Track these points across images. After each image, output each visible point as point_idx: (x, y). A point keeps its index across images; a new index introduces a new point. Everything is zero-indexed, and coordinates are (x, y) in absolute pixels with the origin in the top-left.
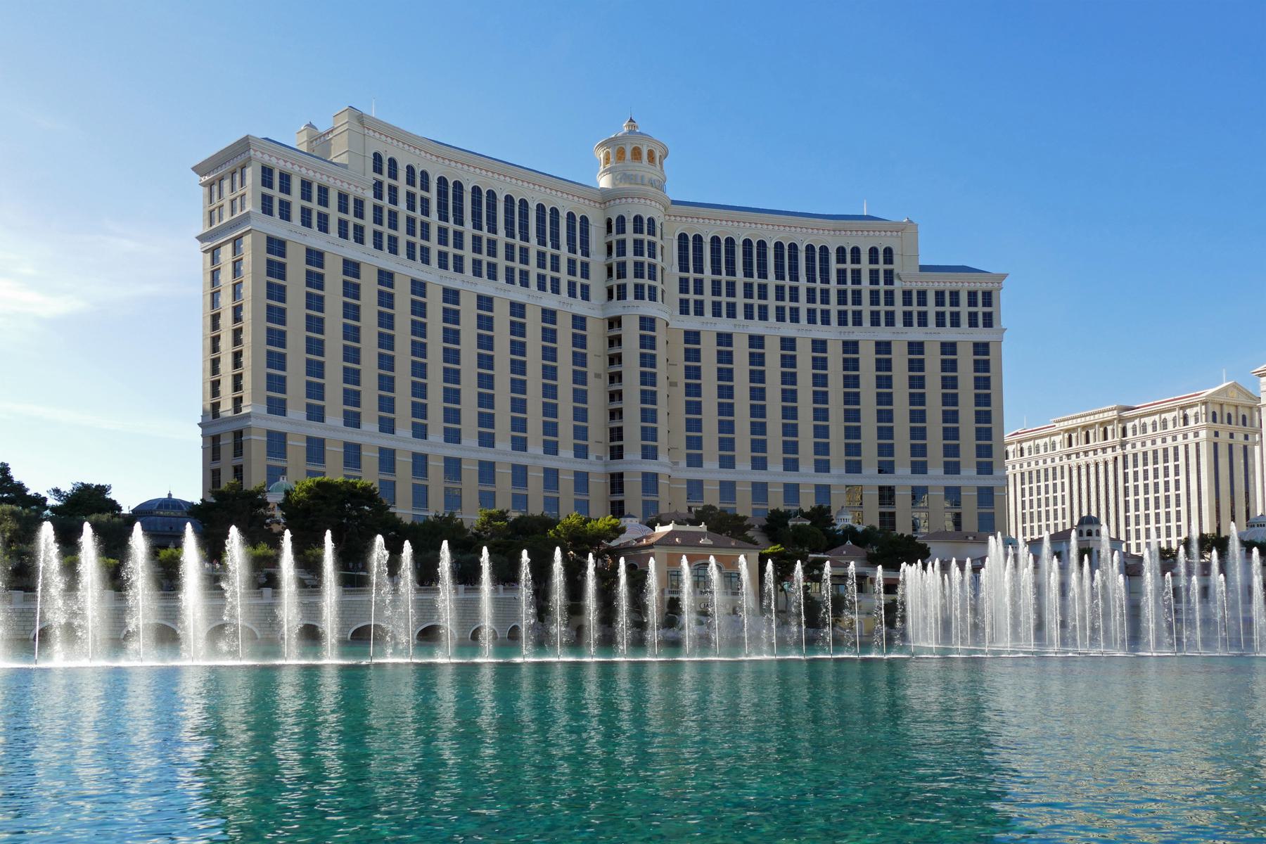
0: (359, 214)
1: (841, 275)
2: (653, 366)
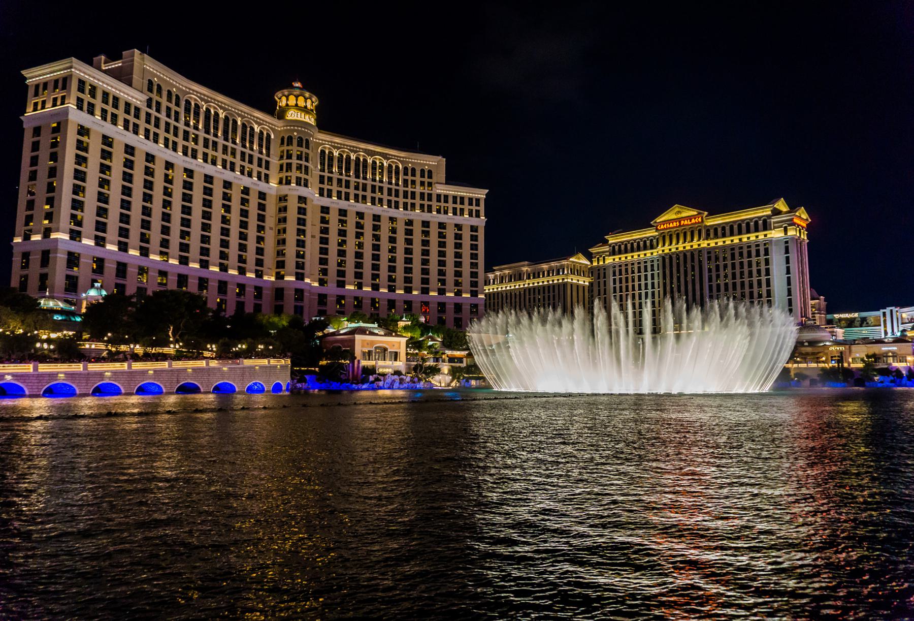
0: (137, 116)
1: (405, 182)
2: (304, 225)
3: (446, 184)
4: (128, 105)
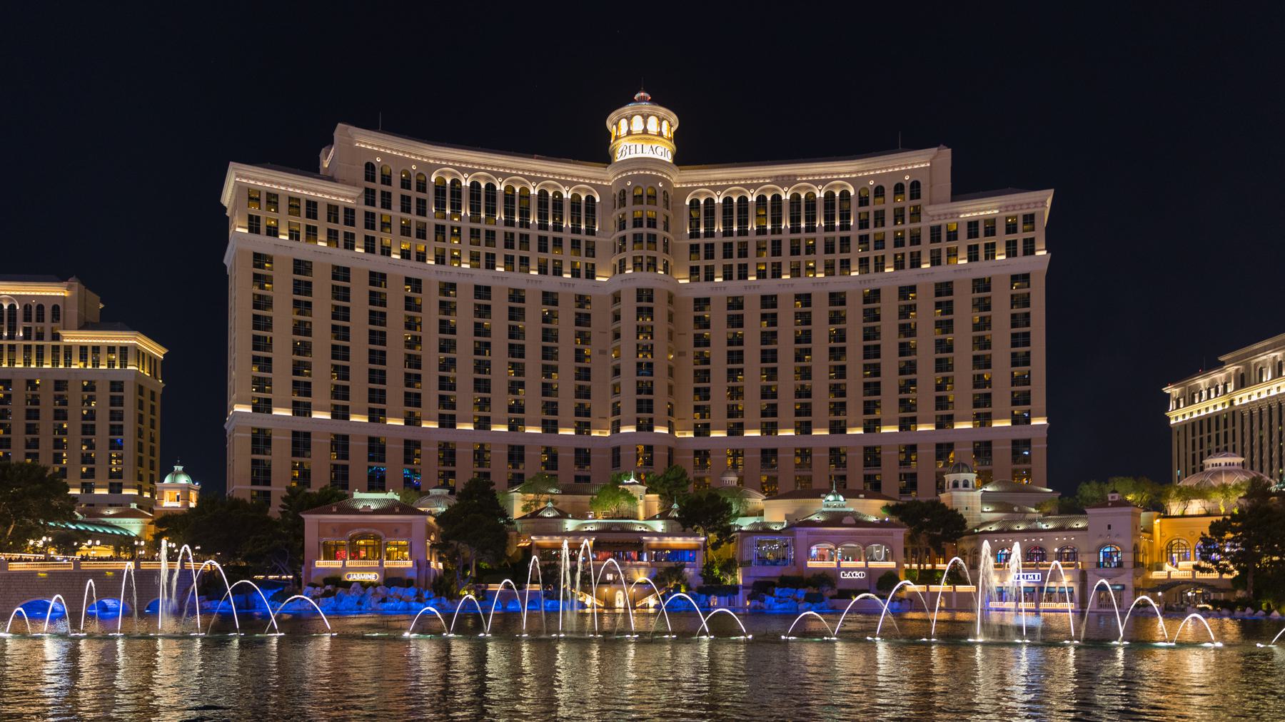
0: (350, 221)
3: (953, 200)
4: (333, 210)
